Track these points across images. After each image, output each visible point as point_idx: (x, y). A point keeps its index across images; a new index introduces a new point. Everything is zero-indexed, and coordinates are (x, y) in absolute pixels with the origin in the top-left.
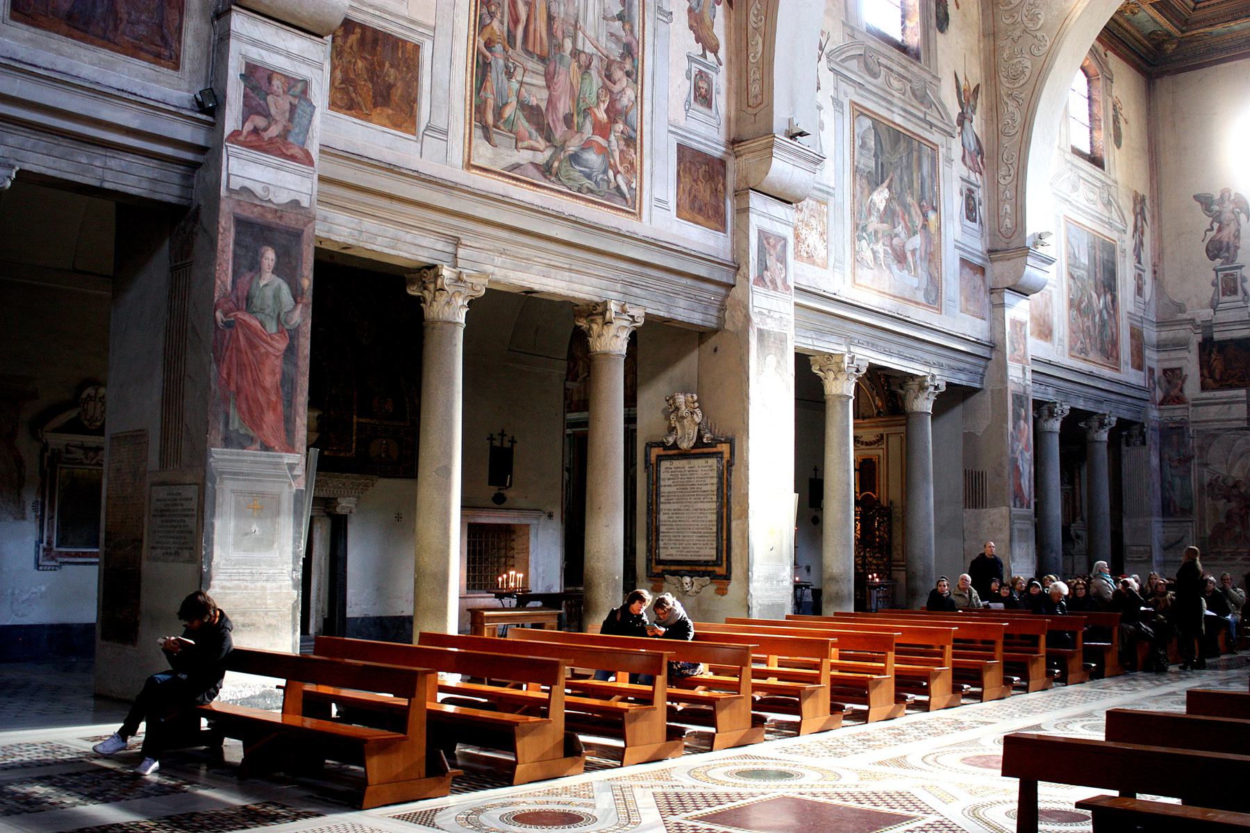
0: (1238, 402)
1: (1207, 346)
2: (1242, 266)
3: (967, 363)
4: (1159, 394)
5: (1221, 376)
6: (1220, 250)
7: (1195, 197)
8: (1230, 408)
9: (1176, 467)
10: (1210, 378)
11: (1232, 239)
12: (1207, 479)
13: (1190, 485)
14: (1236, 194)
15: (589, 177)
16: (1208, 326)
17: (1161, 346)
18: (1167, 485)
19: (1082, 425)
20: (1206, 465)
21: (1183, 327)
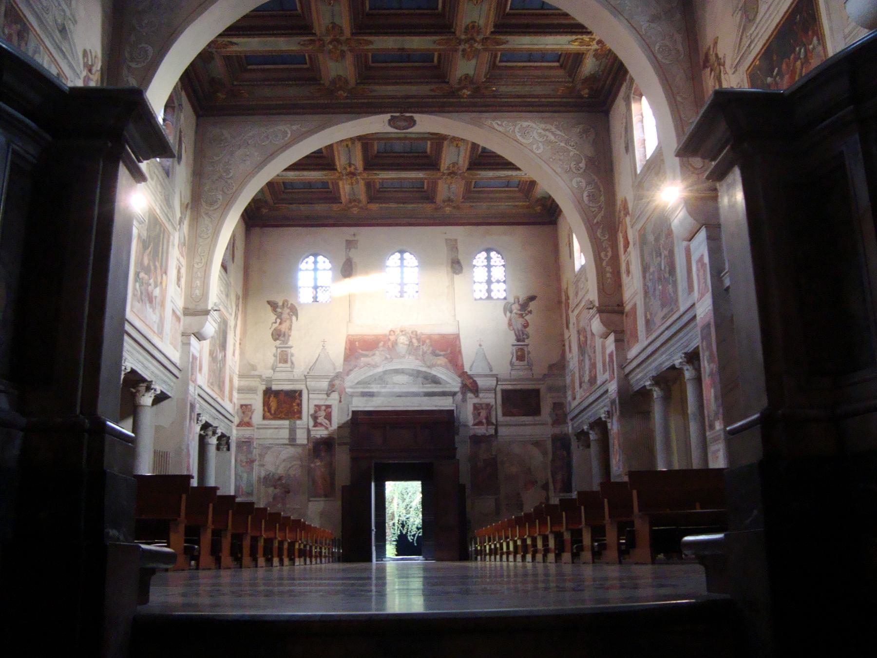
0: (284, 428)
4: (236, 420)
6: (279, 335)
11: (287, 330)
12: (263, 474)
14: (292, 304)
16: (269, 380)
20: (263, 465)
21: (255, 379)
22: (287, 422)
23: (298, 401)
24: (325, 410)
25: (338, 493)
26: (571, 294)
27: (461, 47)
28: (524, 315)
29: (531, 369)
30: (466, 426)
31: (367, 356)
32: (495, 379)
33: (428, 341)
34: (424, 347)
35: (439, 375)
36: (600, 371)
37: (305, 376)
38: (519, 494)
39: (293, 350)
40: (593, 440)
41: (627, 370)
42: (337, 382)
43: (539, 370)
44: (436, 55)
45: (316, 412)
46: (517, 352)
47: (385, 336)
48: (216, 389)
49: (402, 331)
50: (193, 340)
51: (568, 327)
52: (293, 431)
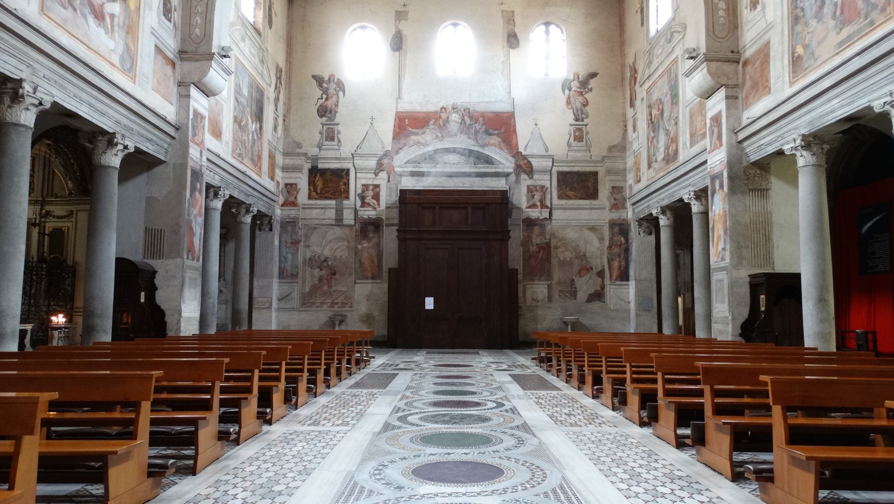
0: (330, 208)
1: (314, 172)
2: (338, 124)
3: (155, 135)
4: (281, 200)
5: (321, 191)
6: (326, 112)
7: (313, 76)
8: (325, 212)
9: (290, 247)
10: (314, 191)
11: (334, 106)
12: (308, 256)
13: (298, 259)
14: (338, 79)
16: (315, 159)
17: (285, 169)
18: (283, 259)
19: (234, 210)
20: (308, 246)
21: (300, 158)
22: (333, 202)
23: (345, 180)
24: (373, 190)
25: (385, 275)
26: (640, 67)
28: (584, 93)
29: (590, 150)
30: (519, 209)
31: (417, 134)
32: (551, 160)
33: (481, 119)
34: (477, 125)
35: (492, 155)
36: (685, 144)
37: (352, 154)
38: (573, 280)
39: (339, 128)
40: (663, 226)
41: (741, 136)
42: (385, 161)
43: (598, 152)
45: (363, 191)
46: (575, 132)
47: (436, 113)
49: (454, 109)
51: (632, 105)
52: (339, 211)
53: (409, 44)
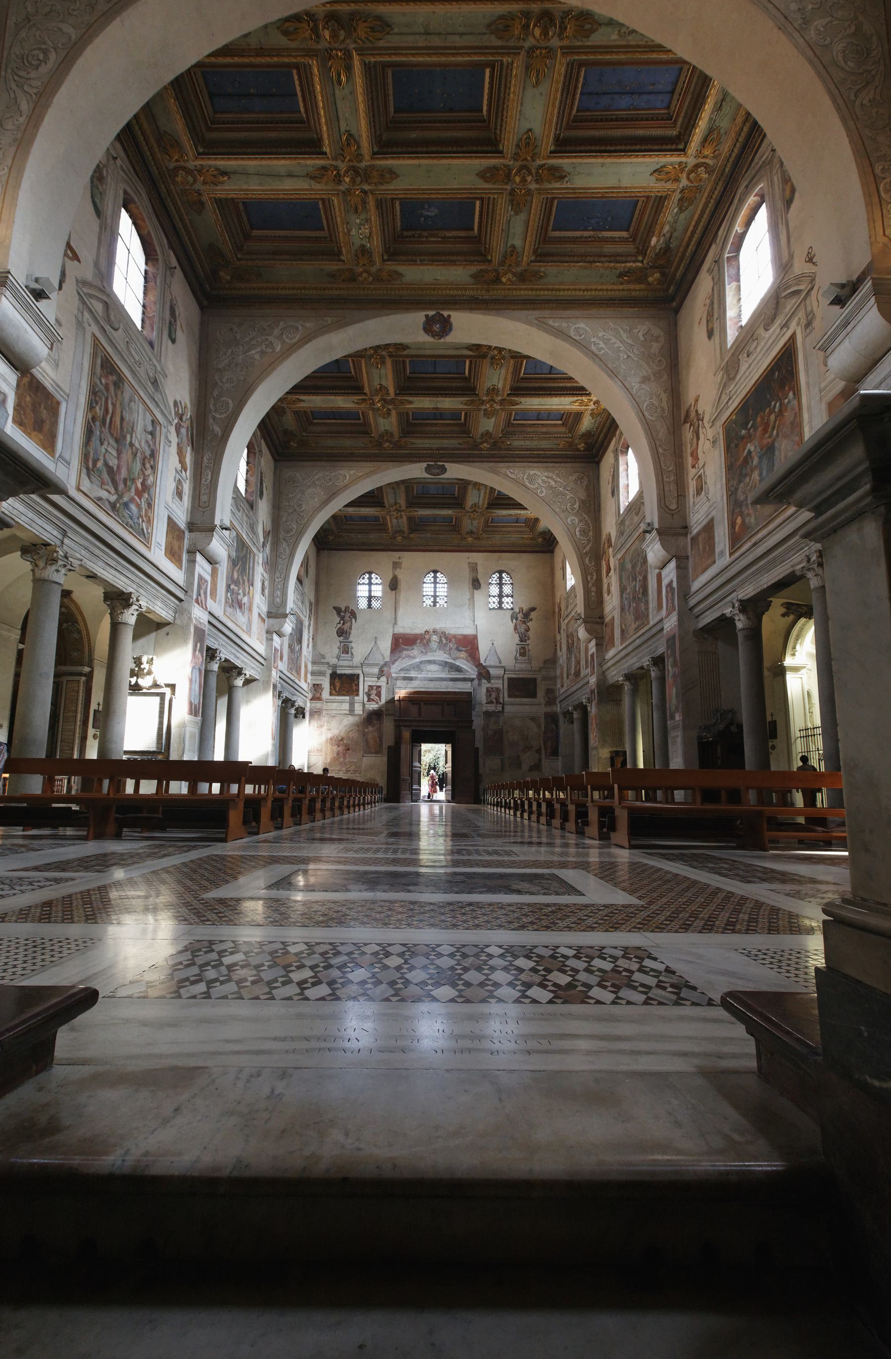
1: (334, 676)
4: (310, 696)
15: (131, 518)
16: (335, 667)
22: (348, 698)
25: (385, 751)
26: (563, 607)
27: (483, 407)
30: (481, 704)
31: (408, 650)
39: (352, 645)
42: (385, 669)
43: (535, 665)
44: (463, 413)
45: (369, 690)
47: (421, 635)
48: (294, 672)
50: (275, 637)
51: (559, 632)
52: (352, 704)
53: (403, 585)
